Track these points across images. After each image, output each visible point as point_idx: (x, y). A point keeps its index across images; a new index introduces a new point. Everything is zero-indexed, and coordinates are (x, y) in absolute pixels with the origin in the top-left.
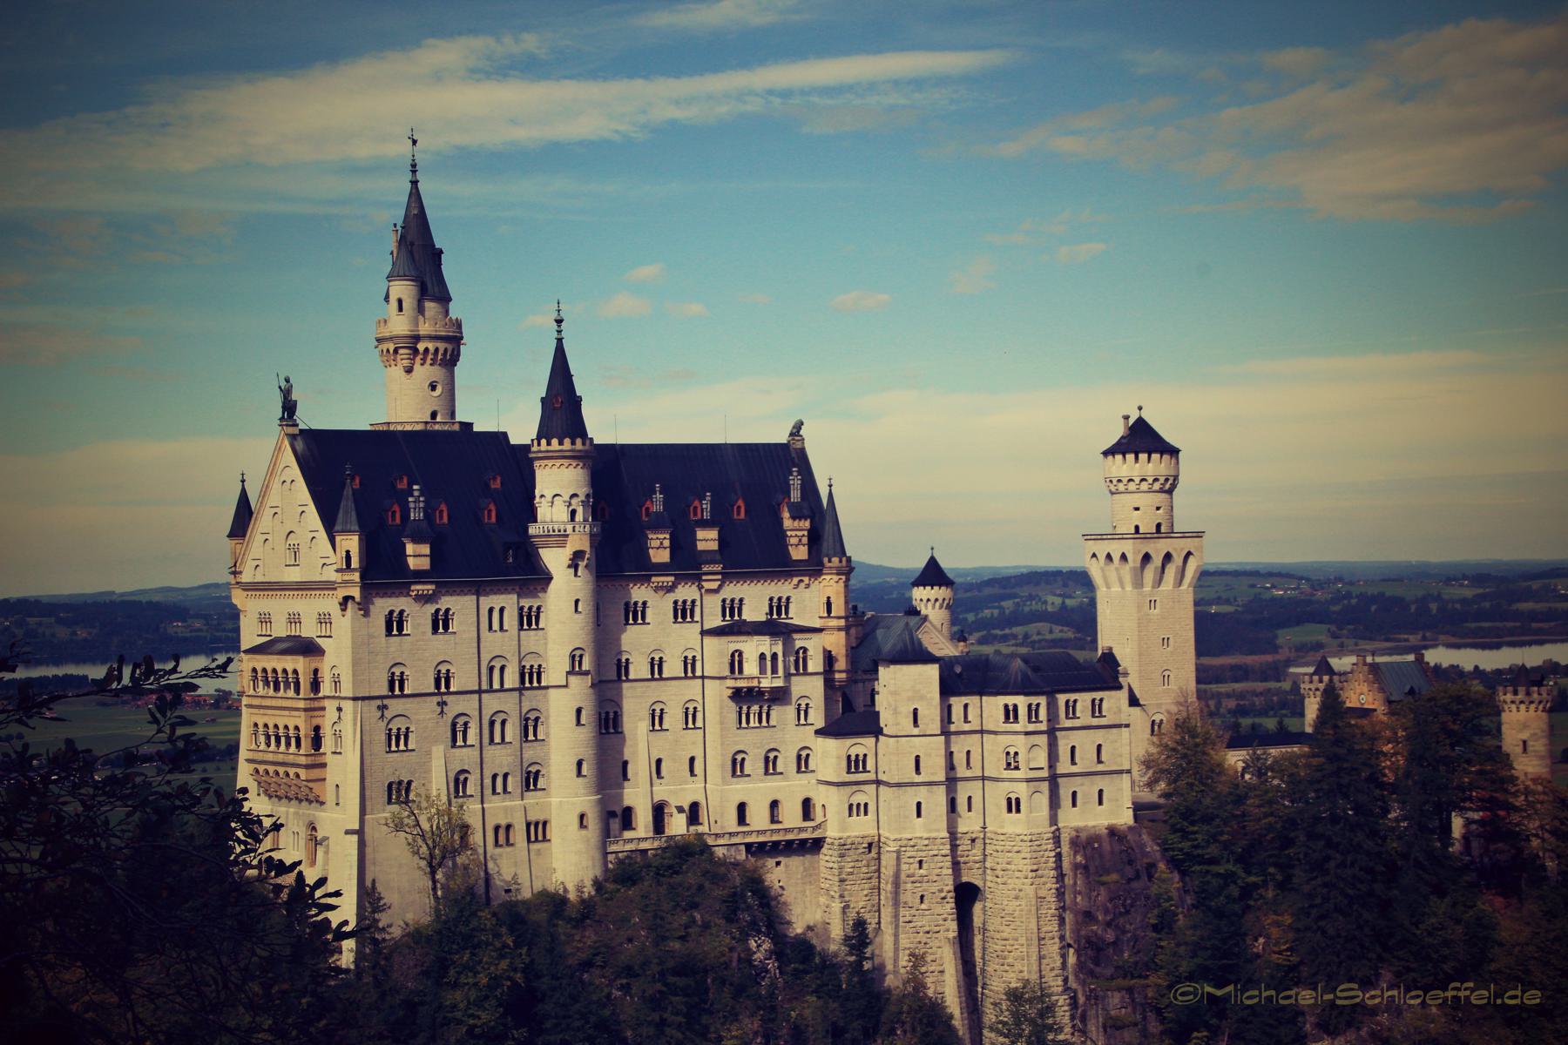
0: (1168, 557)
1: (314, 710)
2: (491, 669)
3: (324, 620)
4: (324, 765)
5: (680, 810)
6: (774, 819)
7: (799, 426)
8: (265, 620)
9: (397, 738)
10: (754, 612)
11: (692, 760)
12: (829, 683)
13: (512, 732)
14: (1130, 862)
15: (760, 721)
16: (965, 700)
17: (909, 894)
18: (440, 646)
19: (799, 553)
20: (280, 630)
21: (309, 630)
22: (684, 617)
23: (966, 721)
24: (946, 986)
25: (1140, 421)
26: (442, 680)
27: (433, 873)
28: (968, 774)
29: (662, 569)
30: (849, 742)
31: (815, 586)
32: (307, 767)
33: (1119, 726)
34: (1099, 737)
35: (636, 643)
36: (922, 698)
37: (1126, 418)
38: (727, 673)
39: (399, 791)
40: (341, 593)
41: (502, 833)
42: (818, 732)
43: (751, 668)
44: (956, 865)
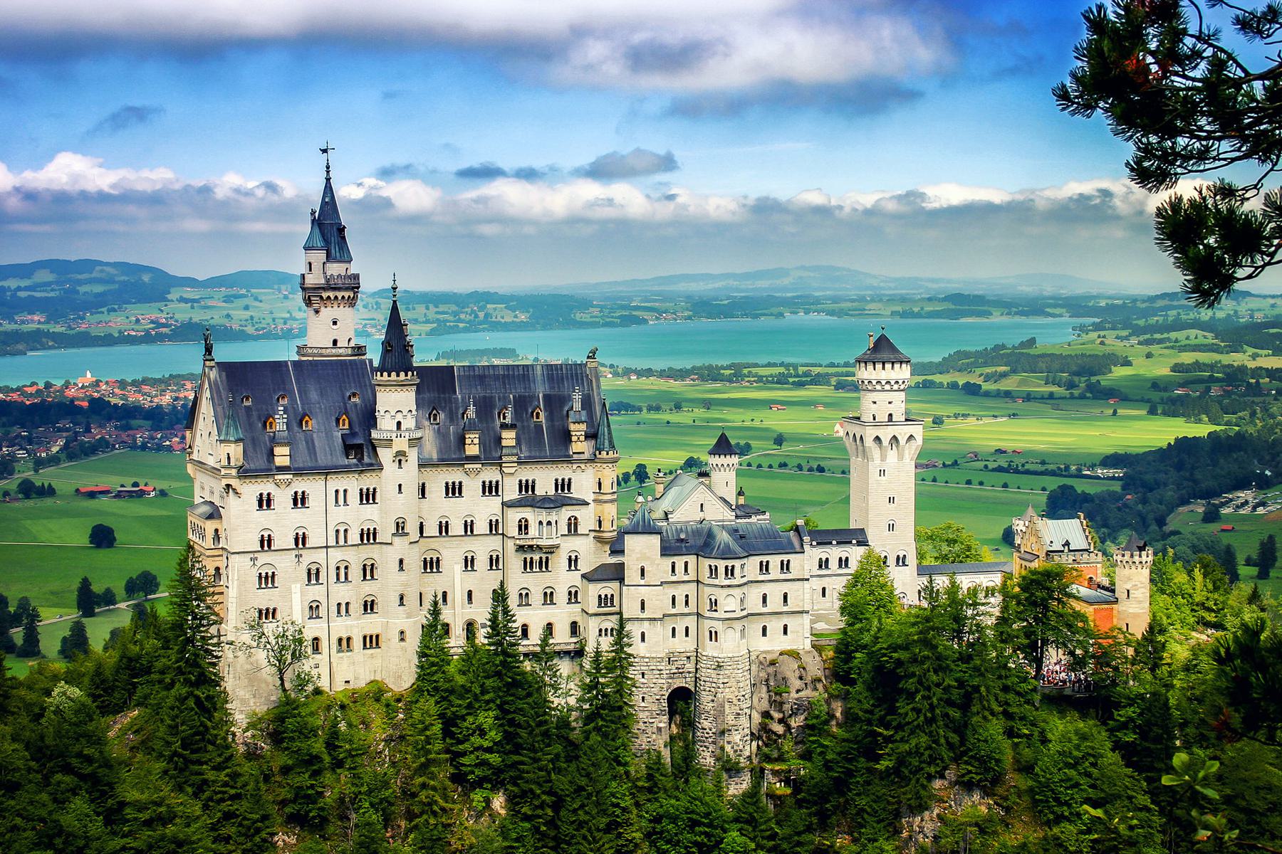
2: (337, 531)
9: (267, 580)
10: (545, 487)
13: (356, 573)
14: (801, 678)
15: (541, 567)
16: (685, 558)
22: (490, 492)
26: (300, 540)
27: (281, 673)
34: (785, 587)
38: (515, 532)
40: (225, 482)
41: (344, 643)
42: (583, 576)
43: (533, 531)
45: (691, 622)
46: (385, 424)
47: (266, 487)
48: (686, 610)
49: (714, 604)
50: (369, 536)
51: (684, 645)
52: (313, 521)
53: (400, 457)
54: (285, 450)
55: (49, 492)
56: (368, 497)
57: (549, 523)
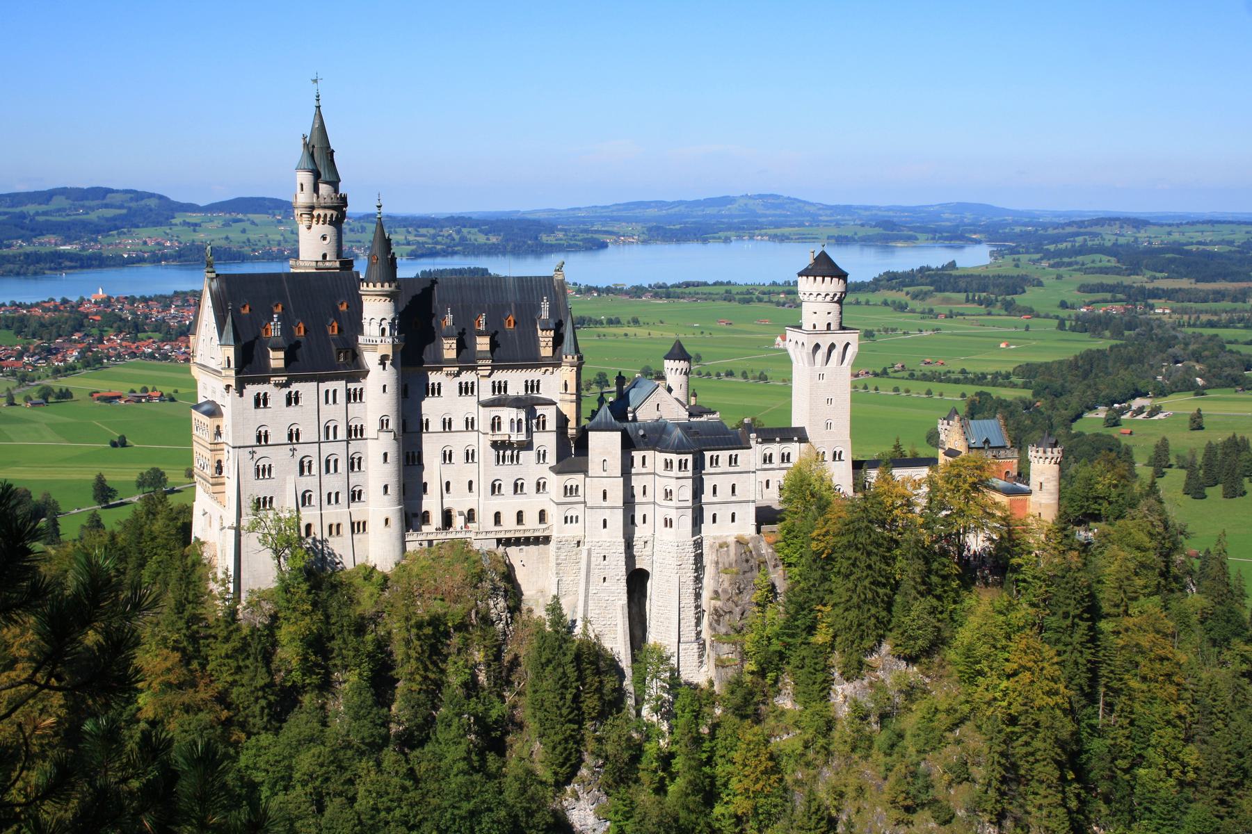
0: (832, 346)
5: (461, 514)
9: (263, 472)
11: (471, 483)
13: (342, 466)
14: (747, 561)
18: (293, 412)
19: (546, 352)
22: (466, 393)
26: (293, 436)
28: (644, 500)
29: (450, 363)
30: (566, 477)
31: (558, 372)
34: (733, 479)
35: (431, 409)
39: (262, 504)
43: (505, 427)
44: (630, 557)
55: (65, 395)
57: (520, 421)
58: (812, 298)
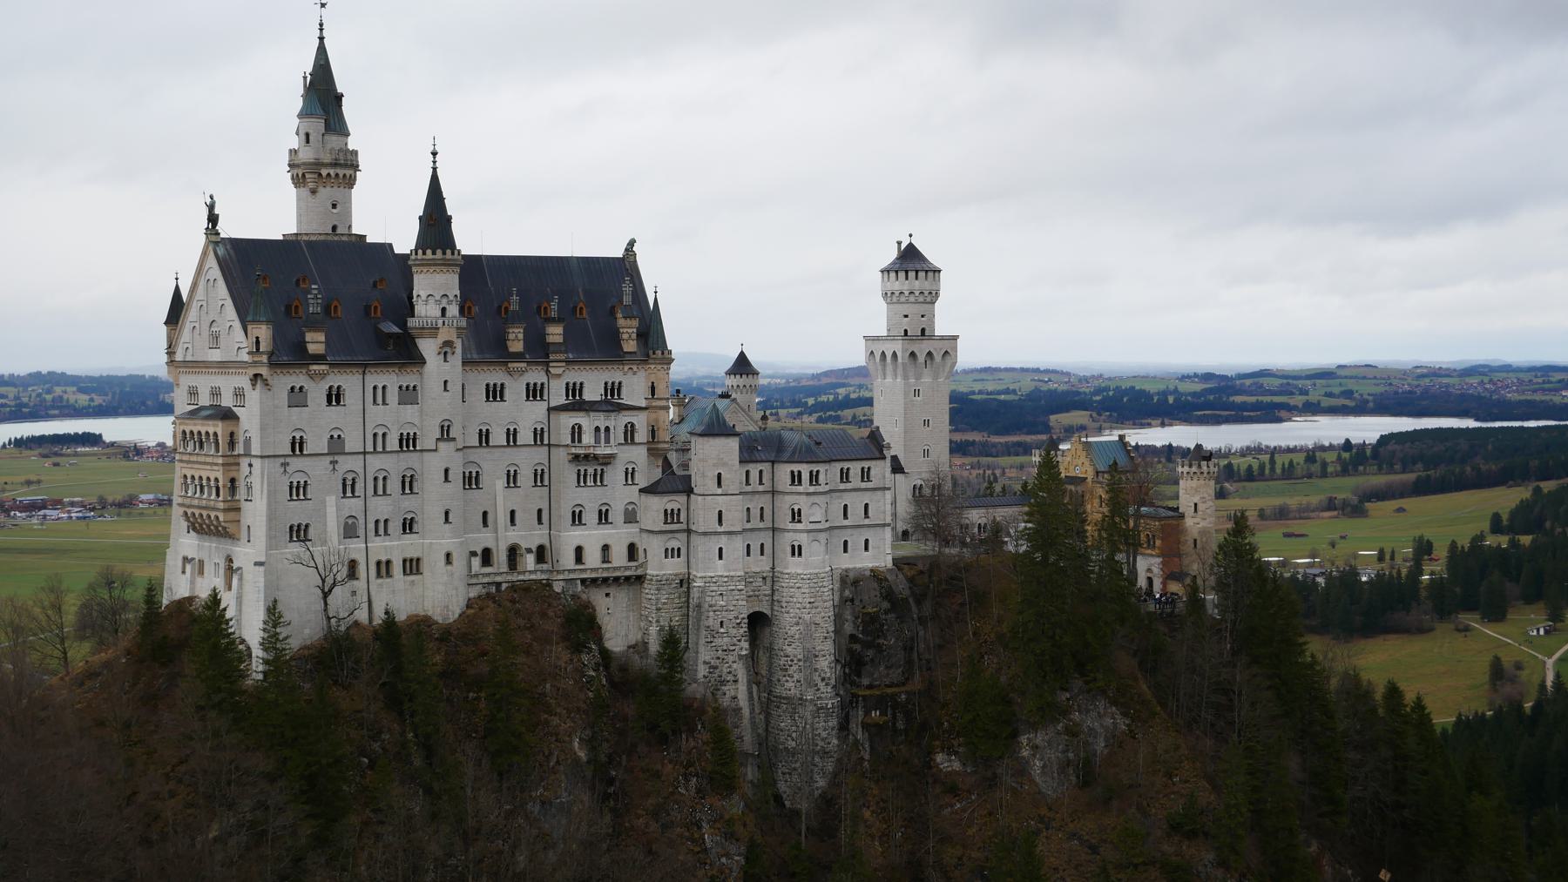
0: (930, 354)
1: (231, 463)
3: (239, 394)
4: (238, 510)
5: (529, 551)
6: (605, 560)
7: (632, 243)
8: (193, 392)
9: (298, 490)
10: (592, 393)
11: (540, 511)
12: (654, 449)
13: (394, 485)
16: (760, 466)
17: (712, 621)
19: (630, 345)
20: (205, 400)
21: (227, 401)
22: (535, 397)
23: (761, 483)
24: (739, 692)
25: (911, 246)
26: (336, 446)
29: (518, 357)
30: (666, 499)
31: (642, 374)
32: (225, 510)
33: (885, 489)
36: (725, 464)
37: (899, 243)
39: (299, 533)
42: (641, 491)
43: (588, 438)
45: (766, 538)
46: (426, 310)
47: (298, 379)
48: (761, 525)
49: (796, 516)
50: (408, 442)
51: (761, 564)
52: (345, 420)
53: (446, 349)
54: (321, 337)
56: (409, 395)
57: (607, 429)
58: (903, 299)
